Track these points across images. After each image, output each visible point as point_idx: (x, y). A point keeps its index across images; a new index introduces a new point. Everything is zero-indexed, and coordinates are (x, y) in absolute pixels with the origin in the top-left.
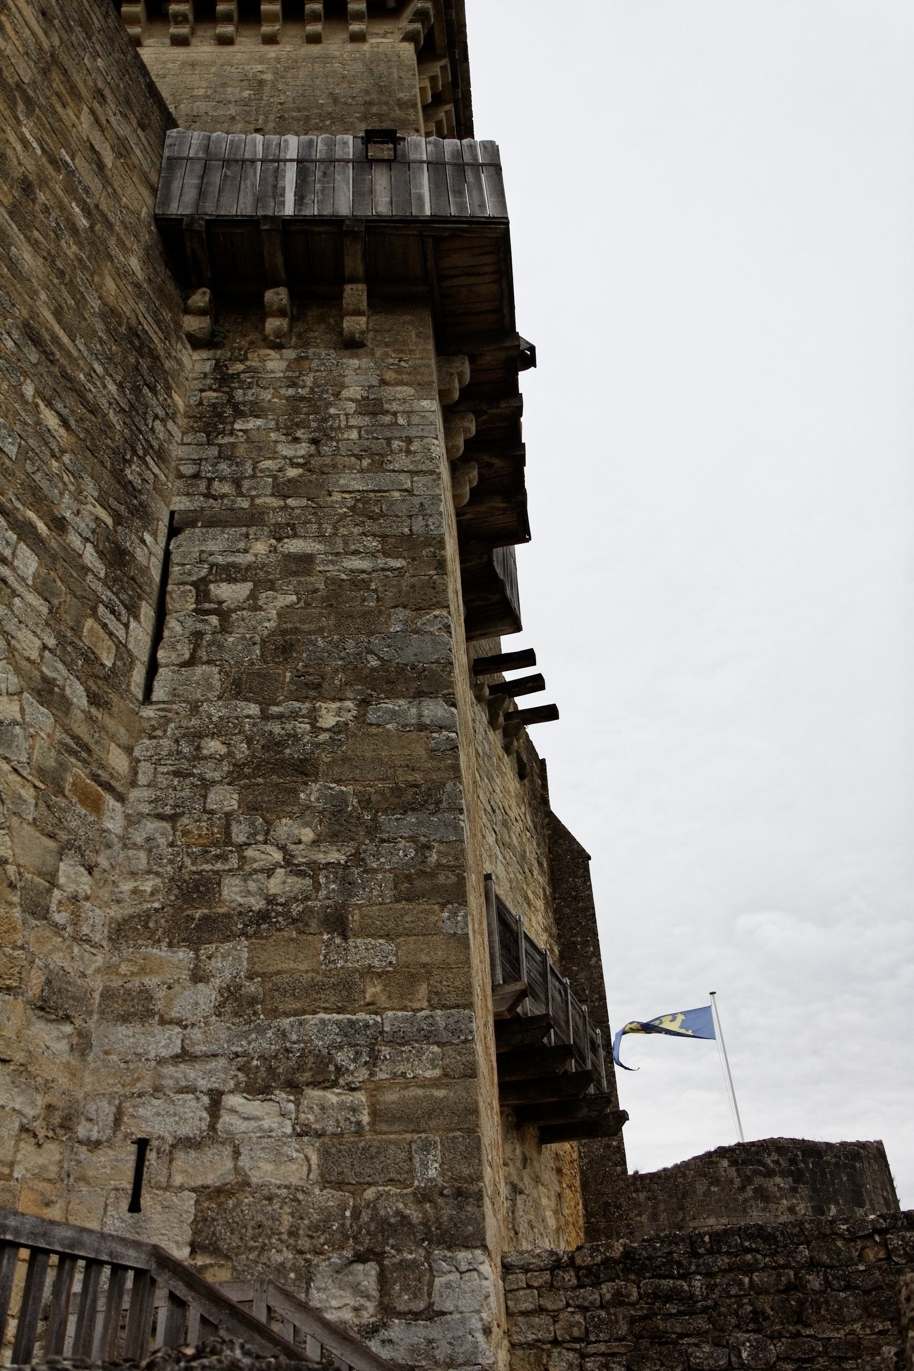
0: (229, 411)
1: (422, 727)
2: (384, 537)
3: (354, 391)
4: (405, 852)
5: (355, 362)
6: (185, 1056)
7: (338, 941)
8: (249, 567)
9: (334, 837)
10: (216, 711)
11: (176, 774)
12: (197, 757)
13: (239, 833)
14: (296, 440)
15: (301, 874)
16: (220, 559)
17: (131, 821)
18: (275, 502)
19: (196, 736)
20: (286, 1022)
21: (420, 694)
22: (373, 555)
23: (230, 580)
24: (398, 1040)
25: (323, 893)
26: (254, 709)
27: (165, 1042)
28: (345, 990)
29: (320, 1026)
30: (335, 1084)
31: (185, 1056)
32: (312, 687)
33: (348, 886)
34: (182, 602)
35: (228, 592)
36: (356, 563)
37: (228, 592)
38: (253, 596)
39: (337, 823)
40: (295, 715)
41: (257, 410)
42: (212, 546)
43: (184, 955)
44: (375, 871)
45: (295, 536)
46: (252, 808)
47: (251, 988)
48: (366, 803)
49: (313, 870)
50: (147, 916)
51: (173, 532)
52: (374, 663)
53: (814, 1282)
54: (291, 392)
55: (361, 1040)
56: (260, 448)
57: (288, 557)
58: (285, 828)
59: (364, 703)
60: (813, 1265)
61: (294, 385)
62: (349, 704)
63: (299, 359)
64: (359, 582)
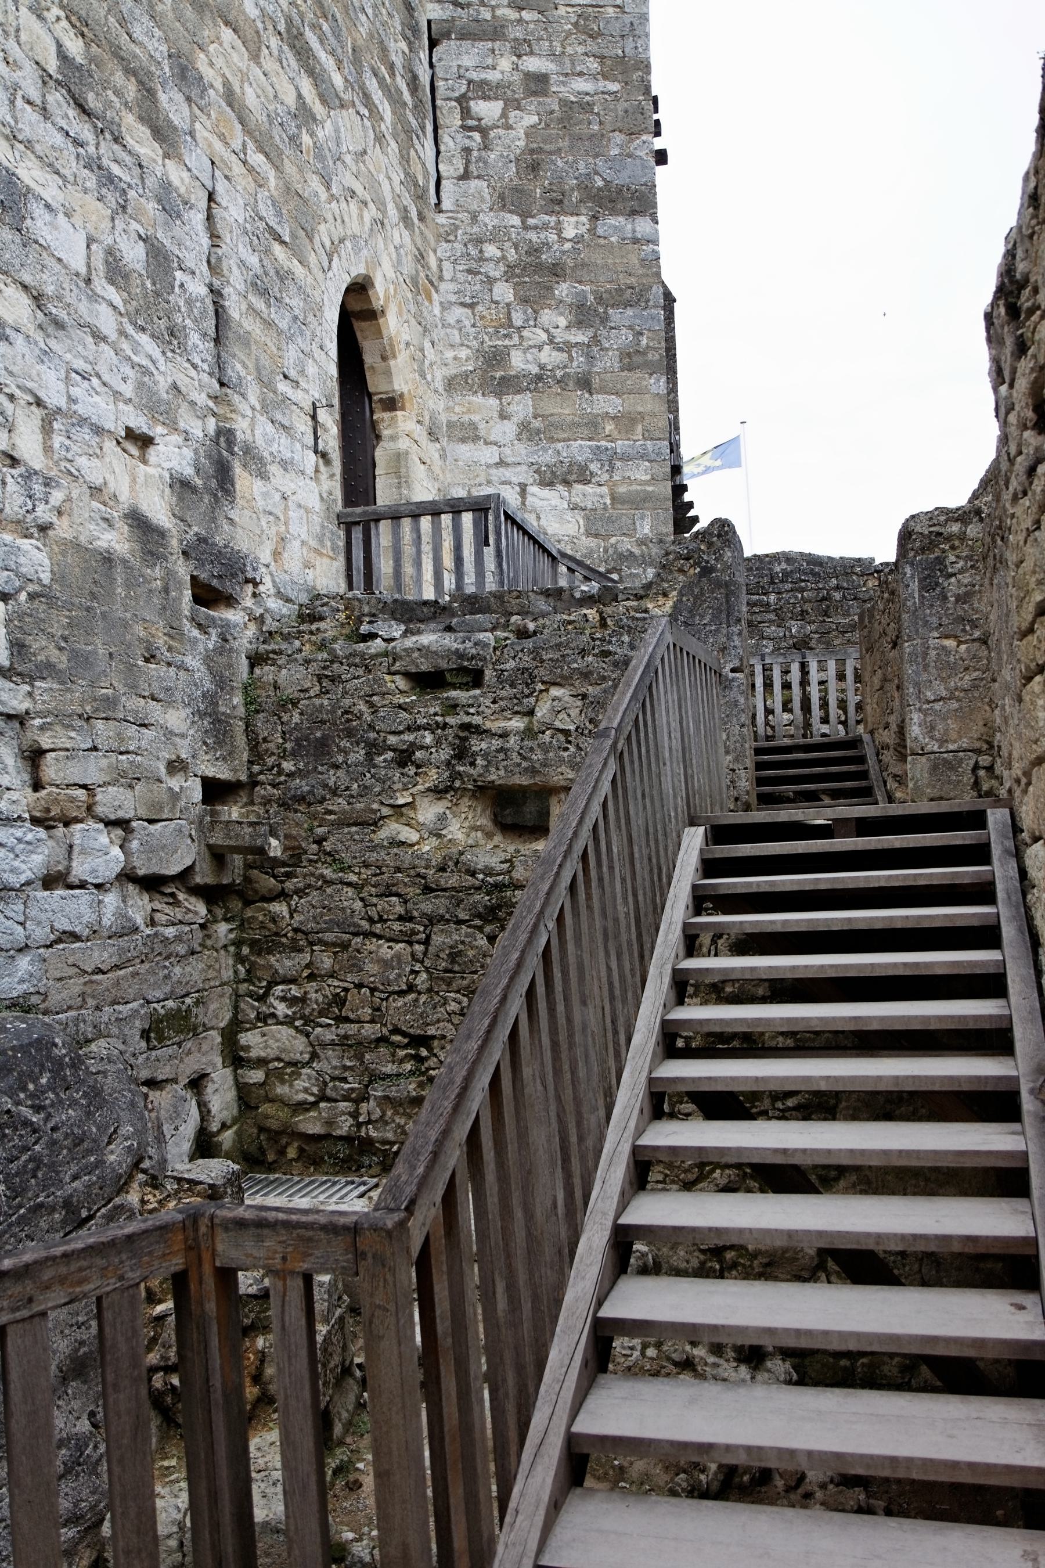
1: (636, 241)
4: (626, 337)
6: (501, 463)
7: (587, 395)
8: (498, 86)
9: (579, 323)
10: (489, 220)
11: (469, 271)
12: (481, 259)
15: (560, 350)
16: (474, 75)
17: (445, 307)
18: (513, 15)
19: (479, 241)
20: (559, 446)
21: (633, 213)
23: (486, 98)
24: (626, 458)
25: (575, 364)
26: (516, 220)
27: (490, 454)
28: (592, 426)
29: (579, 449)
30: (590, 482)
31: (501, 463)
32: (557, 204)
33: (590, 358)
34: (451, 118)
35: (487, 110)
36: (581, 85)
37: (487, 110)
38: (504, 115)
39: (583, 315)
40: (546, 227)
42: (467, 61)
43: (493, 401)
44: (607, 349)
45: (531, 53)
47: (537, 424)
48: (599, 299)
49: (567, 347)
50: (466, 376)
51: (433, 44)
52: (600, 183)
53: (837, 596)
55: (604, 457)
57: (529, 76)
58: (547, 316)
59: (594, 218)
60: (838, 588)
62: (583, 219)
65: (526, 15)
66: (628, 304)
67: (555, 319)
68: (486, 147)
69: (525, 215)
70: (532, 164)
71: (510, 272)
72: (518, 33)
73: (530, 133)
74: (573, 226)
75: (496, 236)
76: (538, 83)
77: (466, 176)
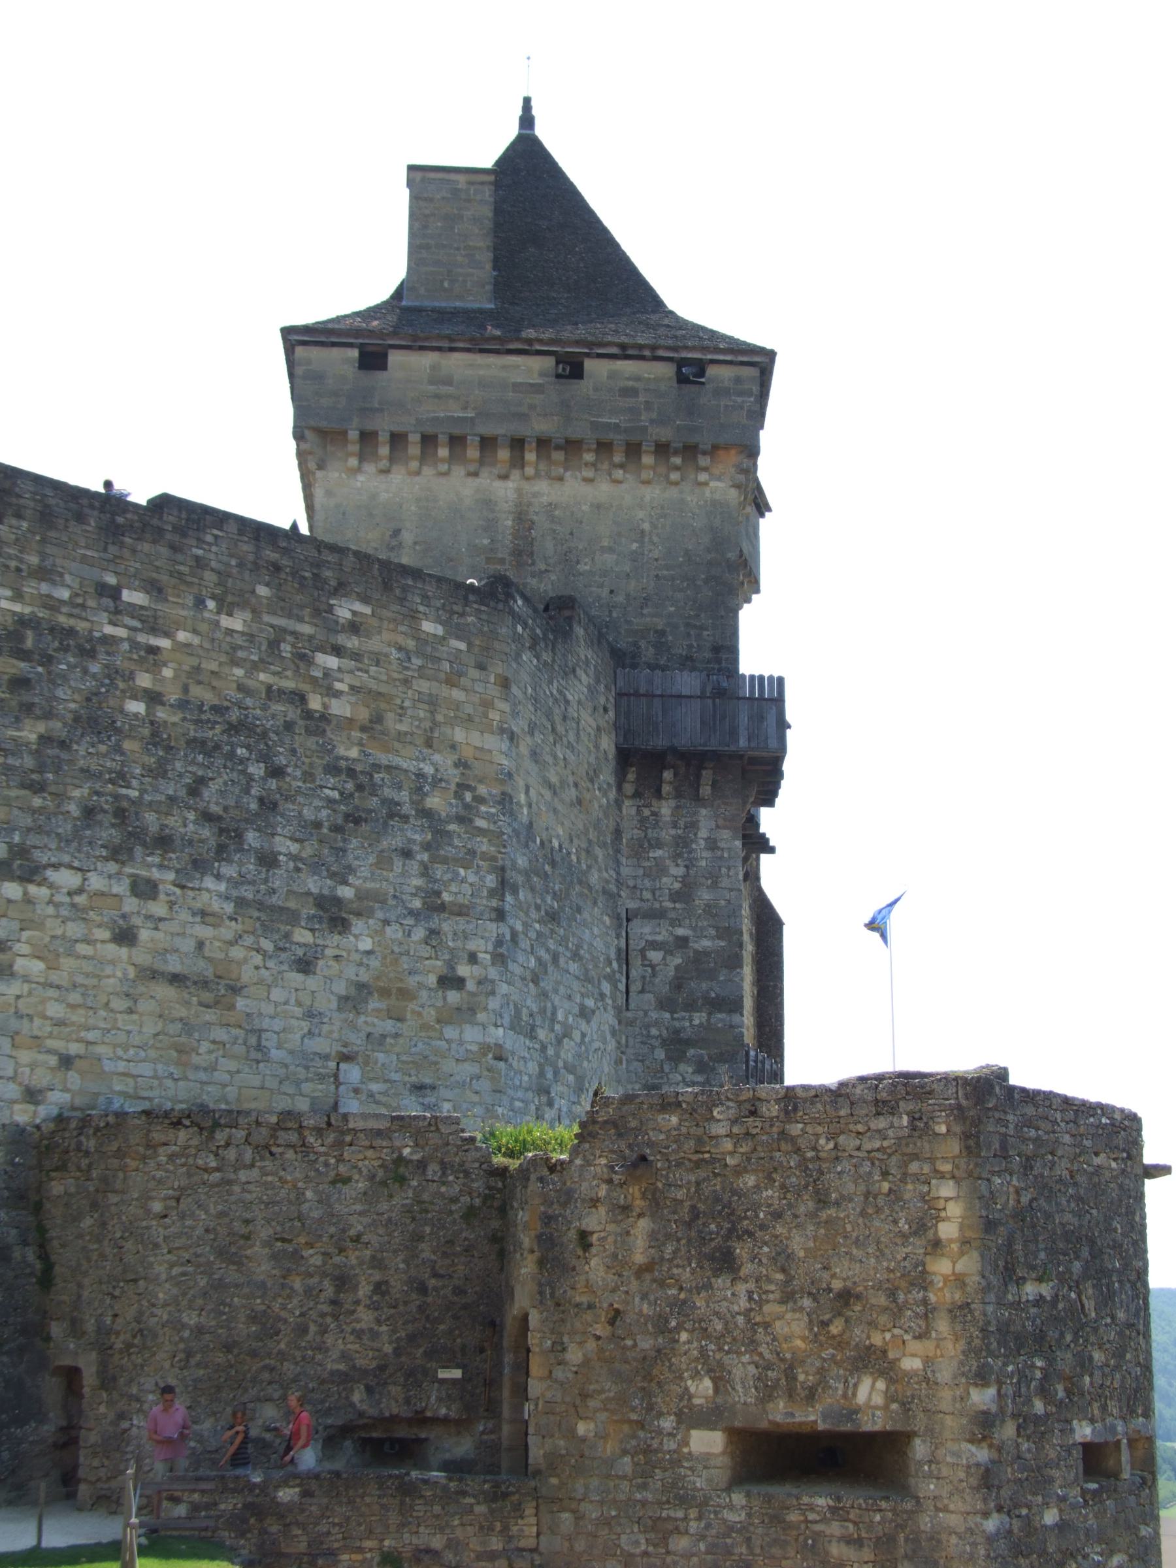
0: (646, 845)
2: (717, 928)
3: (703, 833)
5: (704, 812)
8: (662, 943)
10: (654, 1015)
11: (642, 1043)
12: (649, 1036)
13: (667, 1068)
14: (677, 865)
16: (650, 938)
18: (671, 905)
19: (647, 1027)
22: (712, 938)
23: (655, 949)
26: (667, 1015)
32: (690, 1007)
34: (636, 962)
35: (655, 956)
37: (655, 956)
38: (664, 958)
39: (702, 1067)
40: (683, 1018)
41: (659, 844)
45: (680, 926)
46: (669, 1058)
48: (710, 1058)
51: (628, 920)
52: (713, 995)
54: (673, 832)
56: (662, 871)
57: (678, 938)
58: (683, 1067)
59: (710, 1014)
61: (675, 827)
62: (704, 1014)
63: (678, 807)
64: (706, 953)
65: (678, 905)
66: (726, 1062)
67: (687, 1069)
68: (654, 975)
69: (672, 1012)
70: (678, 984)
71: (664, 1043)
72: (672, 915)
73: (677, 968)
74: (699, 1018)
75: (656, 1023)
76: (683, 942)
77: (642, 991)
